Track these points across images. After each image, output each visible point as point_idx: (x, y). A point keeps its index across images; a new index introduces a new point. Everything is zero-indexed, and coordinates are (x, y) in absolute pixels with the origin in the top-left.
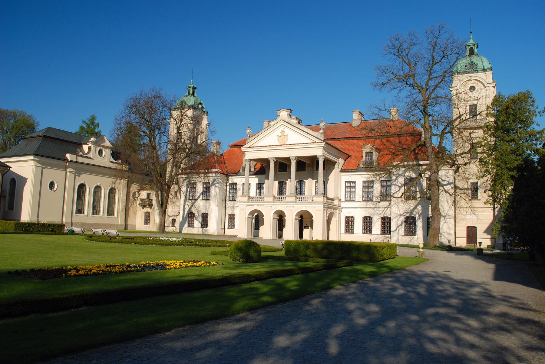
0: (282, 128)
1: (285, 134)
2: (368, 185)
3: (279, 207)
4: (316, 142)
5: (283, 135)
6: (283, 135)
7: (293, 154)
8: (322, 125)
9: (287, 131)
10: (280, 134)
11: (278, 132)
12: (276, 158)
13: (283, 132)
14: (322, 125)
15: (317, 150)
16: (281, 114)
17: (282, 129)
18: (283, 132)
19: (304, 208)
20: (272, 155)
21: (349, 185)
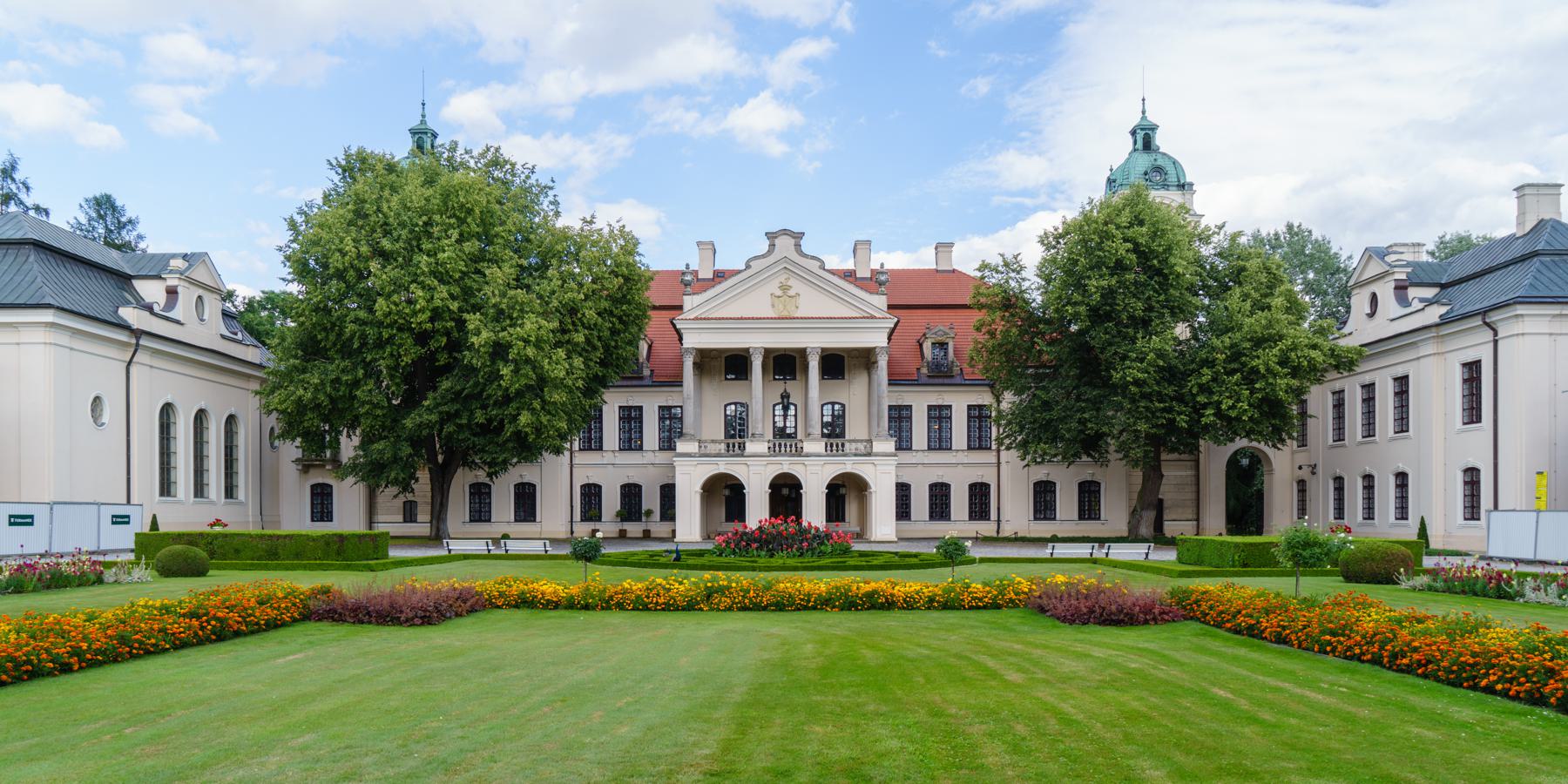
0: (782, 278)
2: (940, 416)
3: (786, 465)
4: (873, 317)
7: (815, 341)
9: (796, 286)
10: (779, 293)
12: (767, 352)
13: (785, 288)
15: (876, 338)
17: (782, 278)
18: (785, 288)
19: (848, 465)
20: (757, 341)
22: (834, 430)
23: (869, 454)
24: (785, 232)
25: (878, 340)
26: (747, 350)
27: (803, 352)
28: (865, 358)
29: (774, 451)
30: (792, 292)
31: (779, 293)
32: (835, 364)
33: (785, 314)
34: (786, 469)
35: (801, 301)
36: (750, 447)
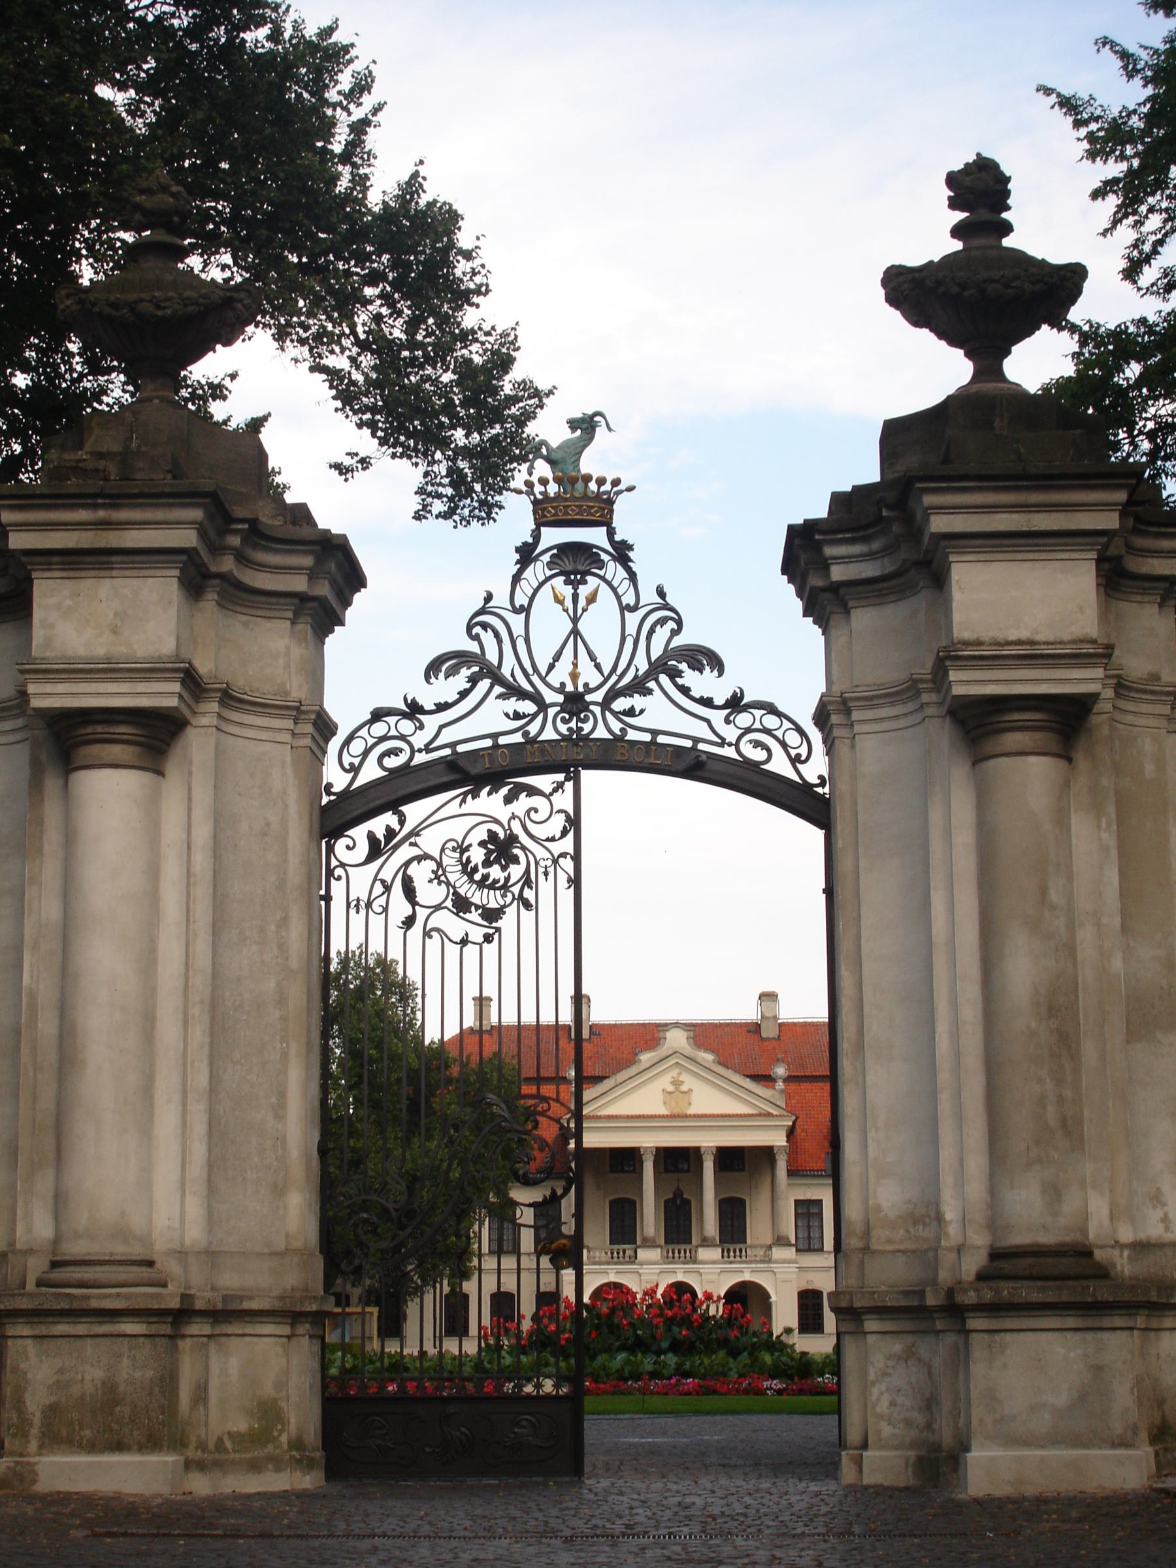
1: (684, 1088)
4: (769, 1115)
5: (677, 1091)
6: (677, 1091)
7: (708, 1140)
8: (780, 1071)
9: (689, 1082)
10: (671, 1088)
11: (665, 1082)
12: (657, 1148)
14: (780, 1071)
16: (668, 1035)
18: (677, 1083)
19: (747, 1277)
20: (648, 1141)
21: (805, 1211)
22: (733, 1231)
23: (770, 1261)
24: (676, 1025)
25: (778, 1139)
26: (639, 1148)
27: (697, 1151)
28: (767, 1153)
29: (668, 1259)
30: (684, 1088)
31: (671, 1088)
32: (729, 1159)
33: (677, 1111)
34: (680, 1277)
35: (694, 1097)
36: (642, 1254)
